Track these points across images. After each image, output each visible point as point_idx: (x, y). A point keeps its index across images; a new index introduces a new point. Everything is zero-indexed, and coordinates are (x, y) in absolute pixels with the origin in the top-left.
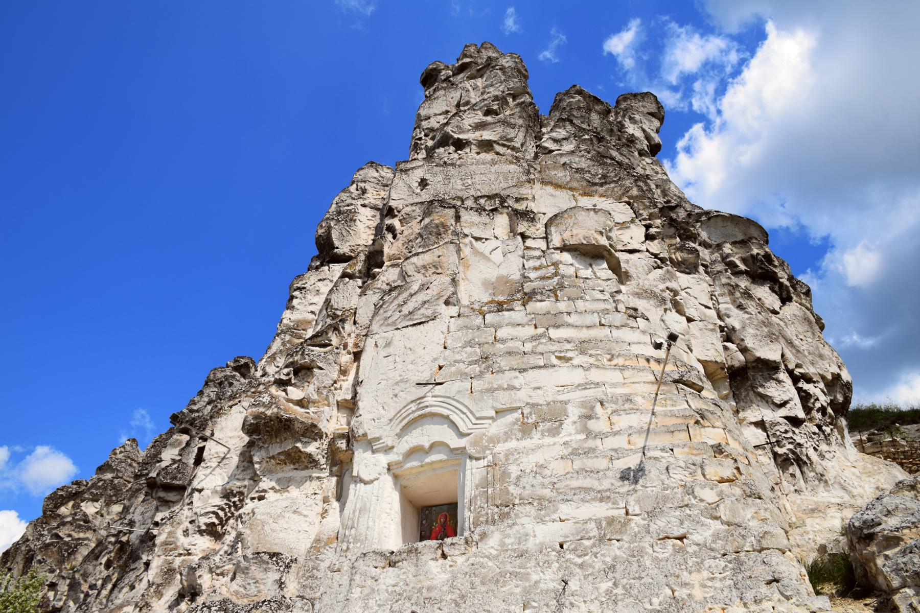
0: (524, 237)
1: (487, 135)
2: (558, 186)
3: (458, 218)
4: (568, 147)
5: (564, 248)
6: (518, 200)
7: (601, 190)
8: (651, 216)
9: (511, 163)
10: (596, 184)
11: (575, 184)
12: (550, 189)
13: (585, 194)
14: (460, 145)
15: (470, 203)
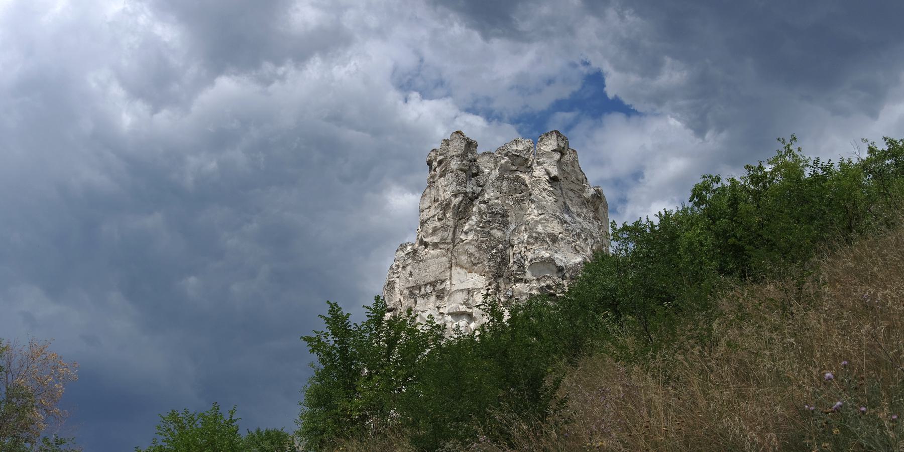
0: (438, 308)
1: (436, 239)
2: (462, 267)
3: (416, 302)
4: (470, 237)
5: (449, 314)
6: (443, 281)
7: (476, 268)
8: (490, 284)
9: (445, 256)
10: (474, 264)
11: (467, 265)
12: (458, 269)
13: (470, 272)
14: (426, 245)
15: (423, 289)
